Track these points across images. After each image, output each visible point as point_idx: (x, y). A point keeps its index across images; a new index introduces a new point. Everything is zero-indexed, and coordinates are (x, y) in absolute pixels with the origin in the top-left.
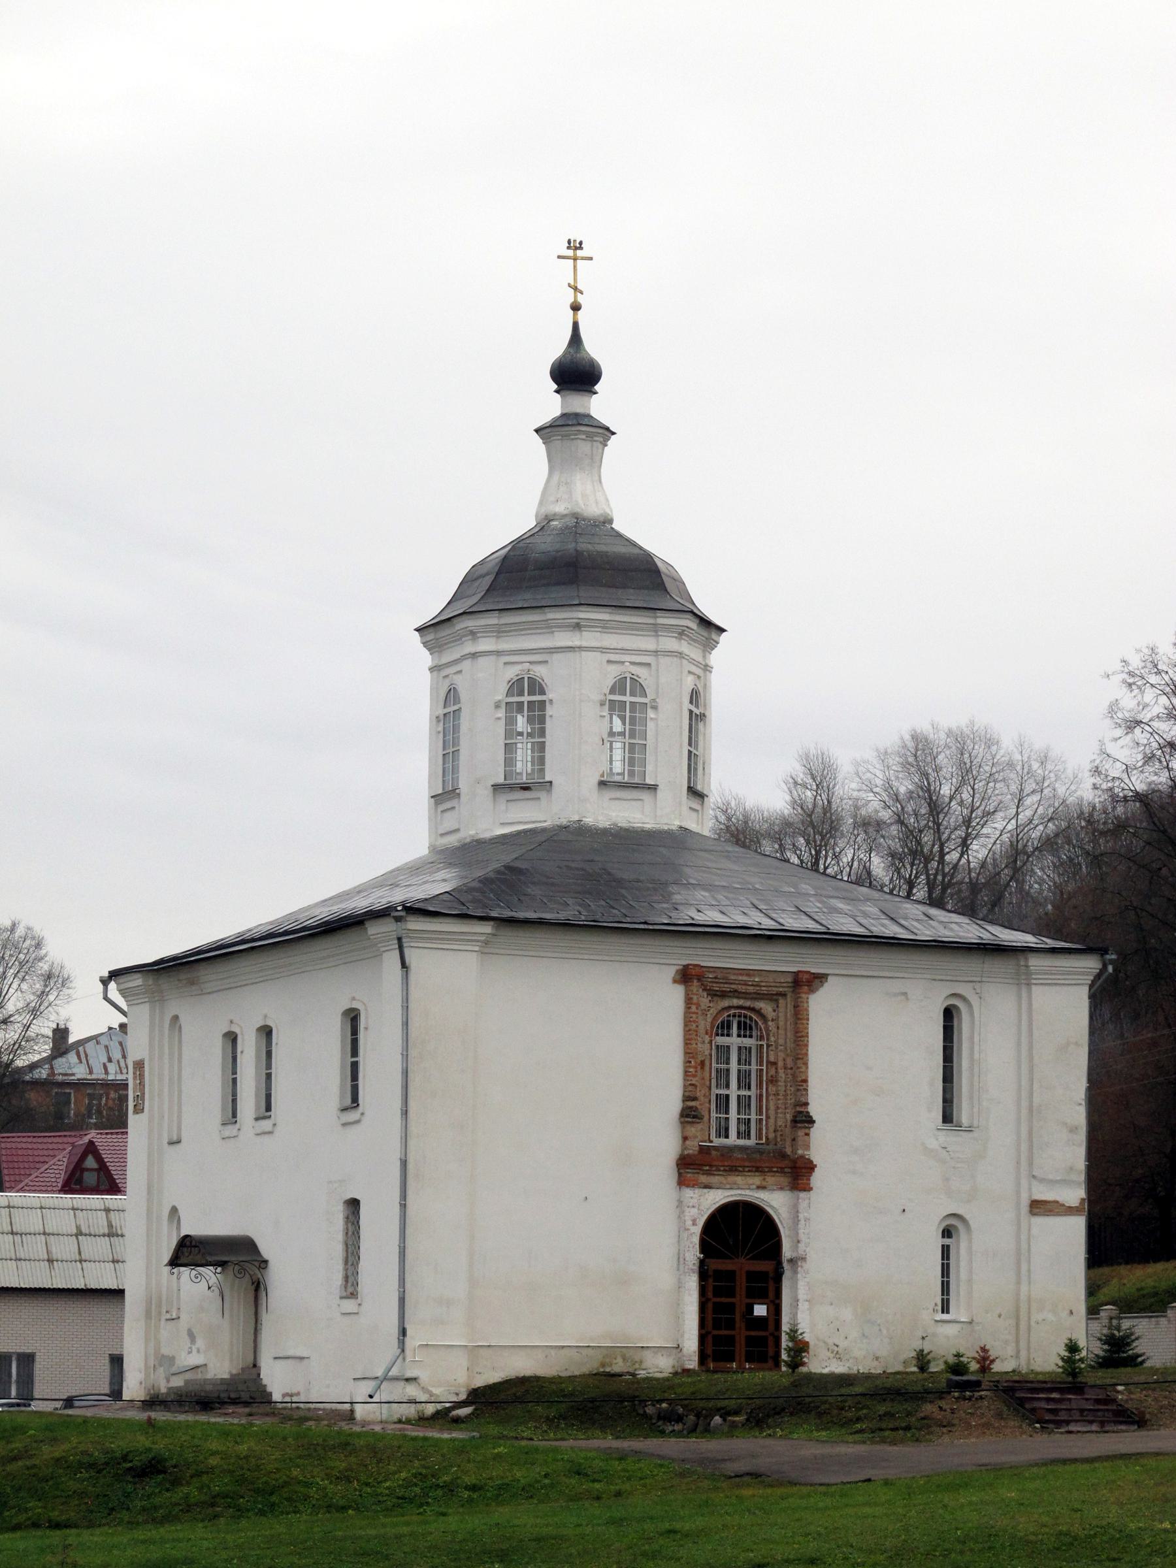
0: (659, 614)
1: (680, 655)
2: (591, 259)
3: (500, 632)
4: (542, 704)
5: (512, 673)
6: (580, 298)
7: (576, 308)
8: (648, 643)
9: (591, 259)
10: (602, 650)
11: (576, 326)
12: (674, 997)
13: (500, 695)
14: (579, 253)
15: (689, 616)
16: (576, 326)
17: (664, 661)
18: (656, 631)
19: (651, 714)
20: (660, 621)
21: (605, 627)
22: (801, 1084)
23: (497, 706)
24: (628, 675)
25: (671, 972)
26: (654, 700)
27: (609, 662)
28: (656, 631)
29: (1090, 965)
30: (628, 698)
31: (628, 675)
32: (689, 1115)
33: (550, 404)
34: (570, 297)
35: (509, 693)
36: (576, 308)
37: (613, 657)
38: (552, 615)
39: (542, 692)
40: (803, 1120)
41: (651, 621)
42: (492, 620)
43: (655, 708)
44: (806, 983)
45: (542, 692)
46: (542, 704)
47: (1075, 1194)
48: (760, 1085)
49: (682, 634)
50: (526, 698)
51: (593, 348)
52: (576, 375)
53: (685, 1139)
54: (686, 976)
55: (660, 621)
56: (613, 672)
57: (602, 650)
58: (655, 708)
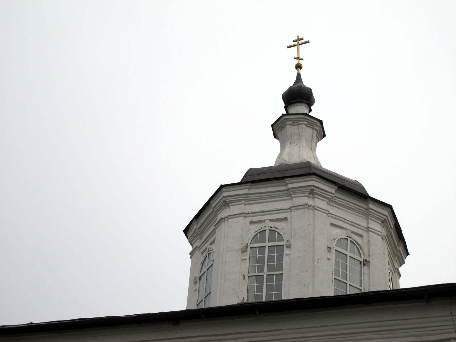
0: (288, 181)
1: (314, 208)
2: (308, 42)
6: (301, 62)
7: (299, 67)
8: (287, 204)
9: (308, 42)
10: (245, 215)
11: (299, 75)
14: (301, 42)
15: (314, 178)
16: (299, 75)
17: (296, 213)
18: (290, 195)
19: (286, 251)
20: (290, 186)
21: (246, 199)
23: (195, 283)
24: (267, 229)
26: (288, 241)
27: (252, 223)
28: (290, 195)
30: (267, 244)
31: (267, 229)
34: (296, 62)
36: (299, 67)
37: (254, 219)
41: (285, 188)
43: (289, 246)
49: (312, 193)
55: (290, 186)
56: (256, 228)
57: (245, 215)
58: (289, 246)
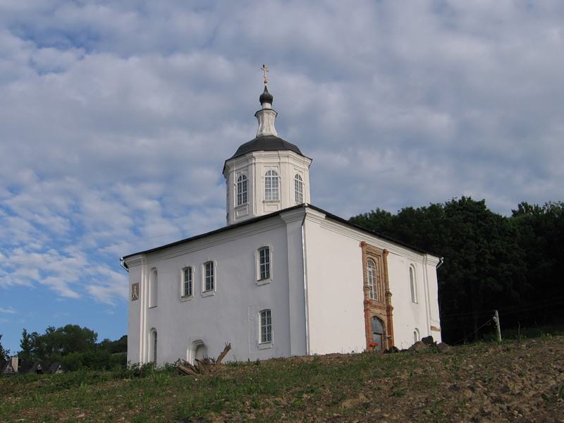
3: (265, 157)
4: (277, 178)
5: (268, 169)
8: (302, 166)
12: (359, 251)
13: (263, 175)
22: (386, 283)
25: (359, 243)
29: (437, 260)
32: (366, 288)
33: (258, 107)
35: (266, 175)
38: (280, 152)
39: (277, 175)
40: (388, 294)
42: (263, 153)
44: (385, 252)
45: (277, 175)
46: (277, 178)
47: (438, 326)
48: (374, 282)
50: (272, 176)
51: (270, 92)
52: (266, 98)
53: (365, 295)
54: (363, 244)
